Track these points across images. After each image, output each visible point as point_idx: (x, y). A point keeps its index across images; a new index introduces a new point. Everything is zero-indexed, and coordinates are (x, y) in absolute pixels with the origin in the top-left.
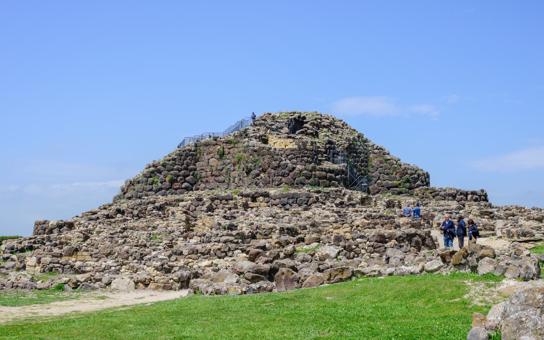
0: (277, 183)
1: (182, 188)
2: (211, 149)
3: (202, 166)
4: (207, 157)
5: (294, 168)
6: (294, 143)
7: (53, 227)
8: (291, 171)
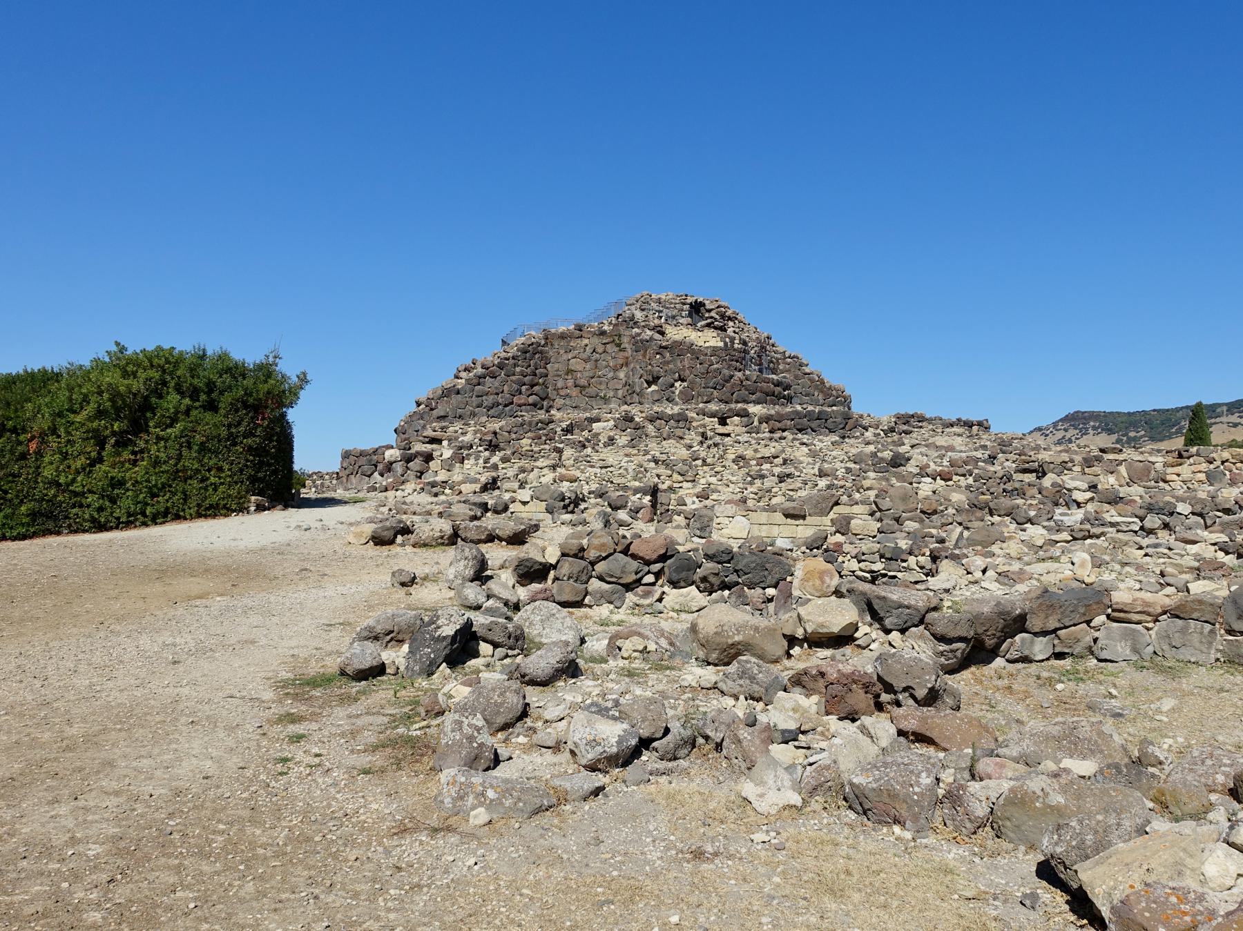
0: (705, 399)
1: (529, 405)
2: (572, 344)
3: (558, 370)
4: (565, 357)
5: (731, 377)
6: (719, 339)
7: (393, 459)
8: (727, 381)
